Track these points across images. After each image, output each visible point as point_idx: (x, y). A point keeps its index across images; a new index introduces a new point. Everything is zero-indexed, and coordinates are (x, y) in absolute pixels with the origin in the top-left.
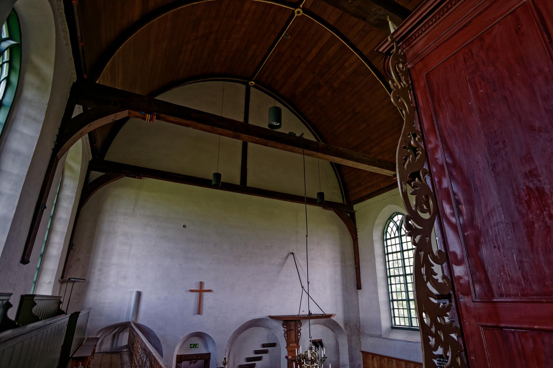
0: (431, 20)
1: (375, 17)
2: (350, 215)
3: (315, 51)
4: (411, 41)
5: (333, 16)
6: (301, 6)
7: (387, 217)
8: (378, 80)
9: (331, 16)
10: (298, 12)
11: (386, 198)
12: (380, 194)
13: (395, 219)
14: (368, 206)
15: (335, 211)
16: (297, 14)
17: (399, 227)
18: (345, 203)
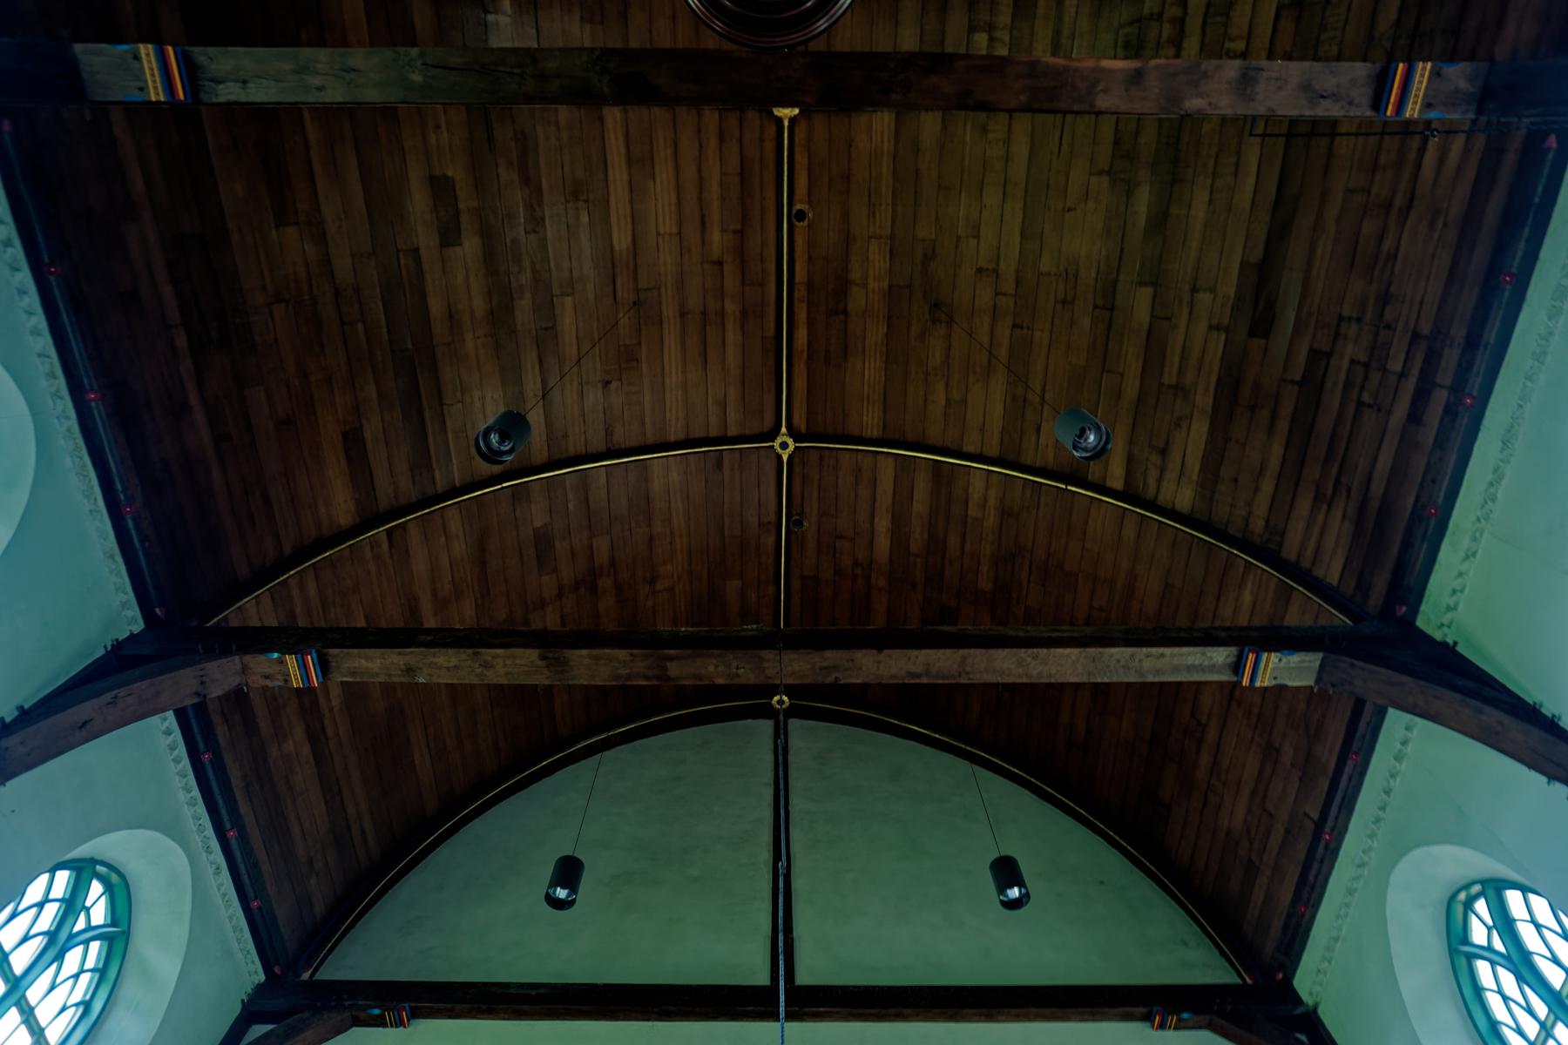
2: (1309, 1039)
3: (883, 524)
5: (867, 416)
6: (784, 430)
7: (1435, 945)
8: (1064, 487)
9: (865, 418)
10: (784, 446)
11: (1364, 852)
12: (1333, 852)
13: (1479, 935)
14: (1336, 940)
15: (1210, 1026)
17: (1515, 956)
18: (1249, 981)
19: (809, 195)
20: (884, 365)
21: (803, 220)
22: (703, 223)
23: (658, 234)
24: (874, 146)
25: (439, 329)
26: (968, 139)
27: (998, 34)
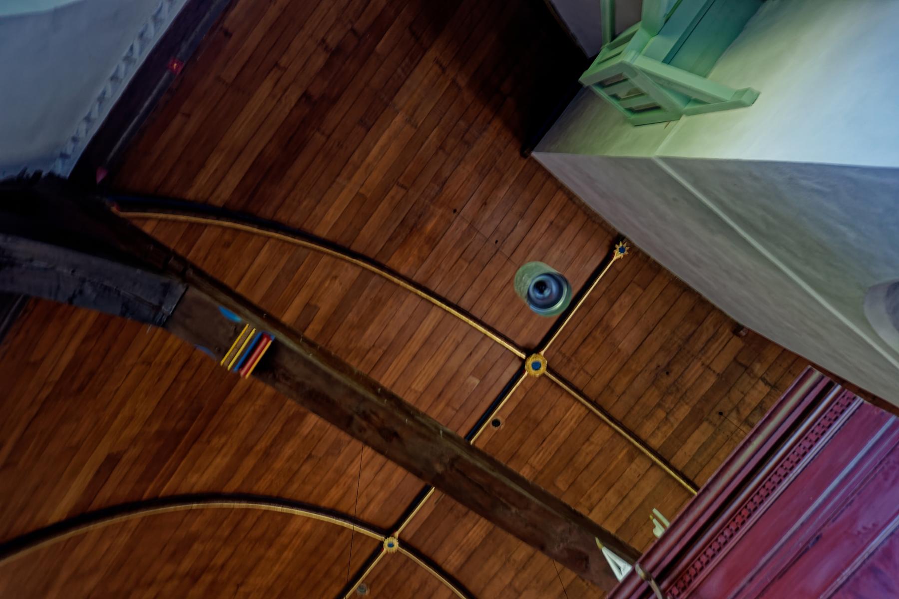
0: (719, 532)
1: (562, 545)
4: (687, 578)
6: (397, 534)
9: (451, 557)
10: (391, 545)
16: (388, 548)
19: (510, 416)
20: (484, 536)
21: (496, 426)
22: (440, 395)
23: (409, 388)
24: (566, 417)
25: (234, 395)
26: (620, 457)
27: (672, 419)
